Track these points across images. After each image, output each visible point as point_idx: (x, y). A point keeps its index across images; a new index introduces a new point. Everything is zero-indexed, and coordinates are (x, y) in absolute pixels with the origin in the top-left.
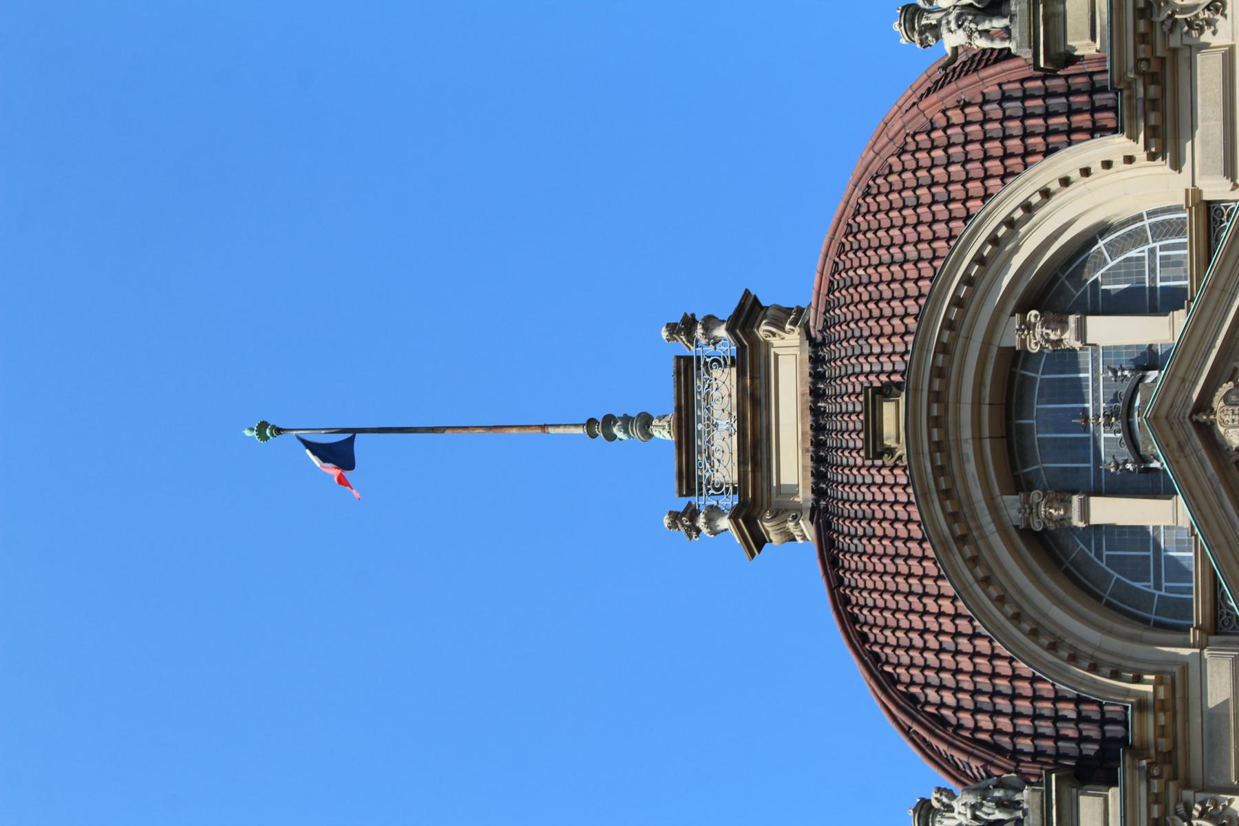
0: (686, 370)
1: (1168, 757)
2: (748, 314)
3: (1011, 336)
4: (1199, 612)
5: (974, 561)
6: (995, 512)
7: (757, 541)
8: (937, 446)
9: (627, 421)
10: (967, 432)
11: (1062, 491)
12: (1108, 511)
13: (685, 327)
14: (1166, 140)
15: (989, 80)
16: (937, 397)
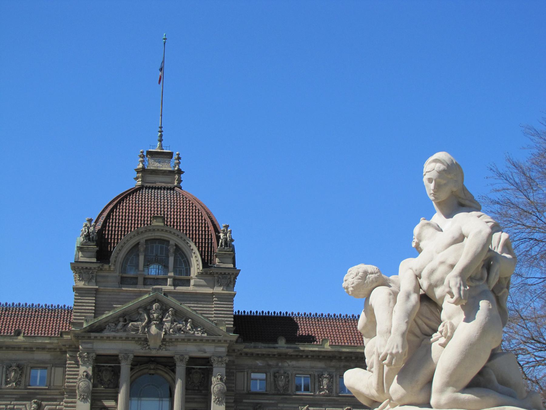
0: (170, 155)
1: (101, 270)
2: (180, 172)
3: (172, 242)
4: (125, 275)
5: (134, 236)
6: (142, 238)
7: (138, 172)
8: (154, 230)
9: (161, 136)
10: (156, 234)
11: (146, 250)
12: (142, 258)
13: (179, 158)
14: (200, 275)
15: (214, 240)
16: (162, 230)
